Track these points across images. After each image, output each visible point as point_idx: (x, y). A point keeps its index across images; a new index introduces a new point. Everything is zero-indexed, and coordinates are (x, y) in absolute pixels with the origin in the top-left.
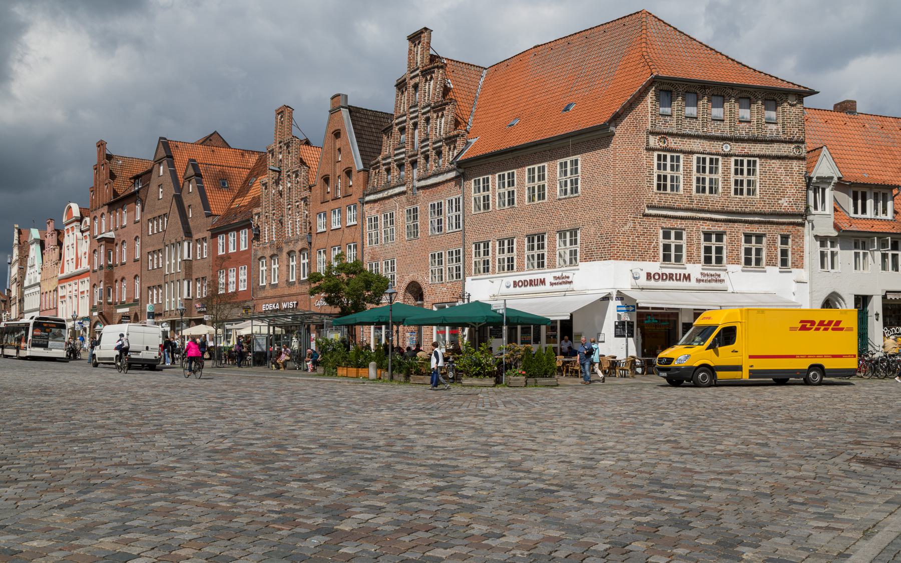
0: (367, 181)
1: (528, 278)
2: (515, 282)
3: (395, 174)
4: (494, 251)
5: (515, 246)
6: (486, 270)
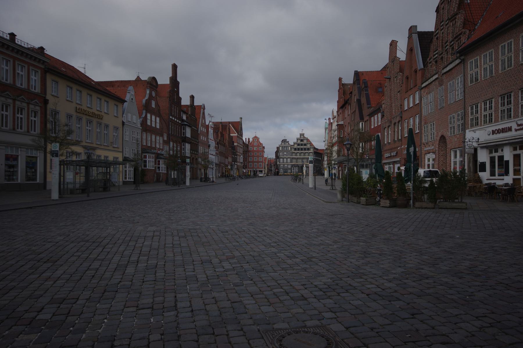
0: (423, 76)
1: (500, 127)
2: (493, 131)
3: (434, 68)
4: (481, 110)
5: (493, 105)
6: (477, 124)
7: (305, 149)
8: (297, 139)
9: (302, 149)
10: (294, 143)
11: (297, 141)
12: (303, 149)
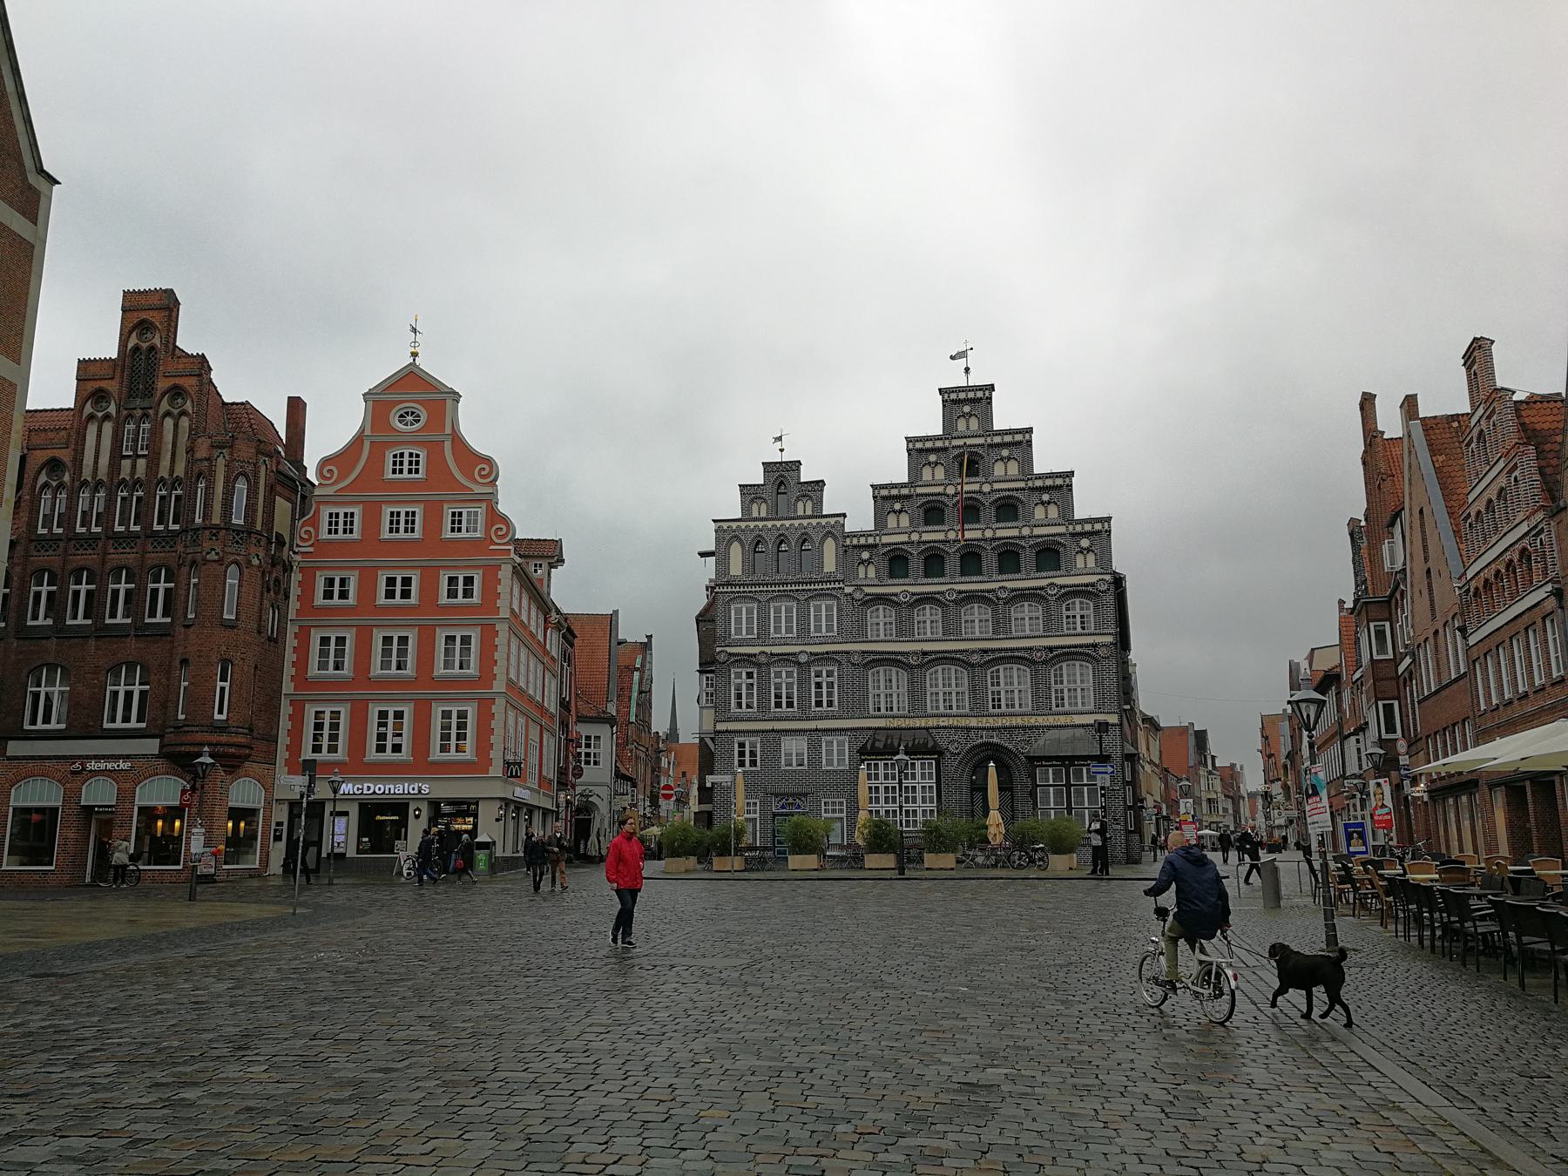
7: (1009, 558)
8: (919, 450)
9: (971, 560)
10: (886, 498)
11: (915, 470)
12: (990, 561)
